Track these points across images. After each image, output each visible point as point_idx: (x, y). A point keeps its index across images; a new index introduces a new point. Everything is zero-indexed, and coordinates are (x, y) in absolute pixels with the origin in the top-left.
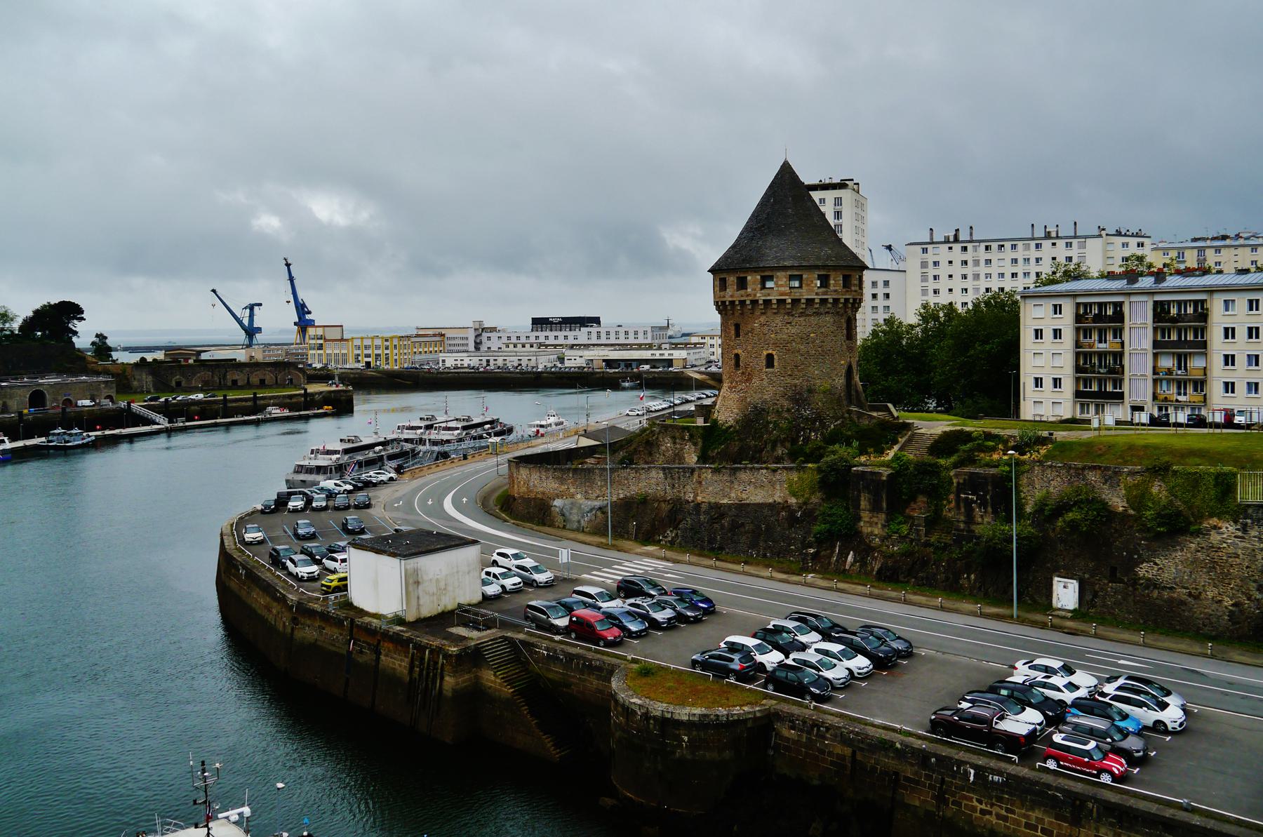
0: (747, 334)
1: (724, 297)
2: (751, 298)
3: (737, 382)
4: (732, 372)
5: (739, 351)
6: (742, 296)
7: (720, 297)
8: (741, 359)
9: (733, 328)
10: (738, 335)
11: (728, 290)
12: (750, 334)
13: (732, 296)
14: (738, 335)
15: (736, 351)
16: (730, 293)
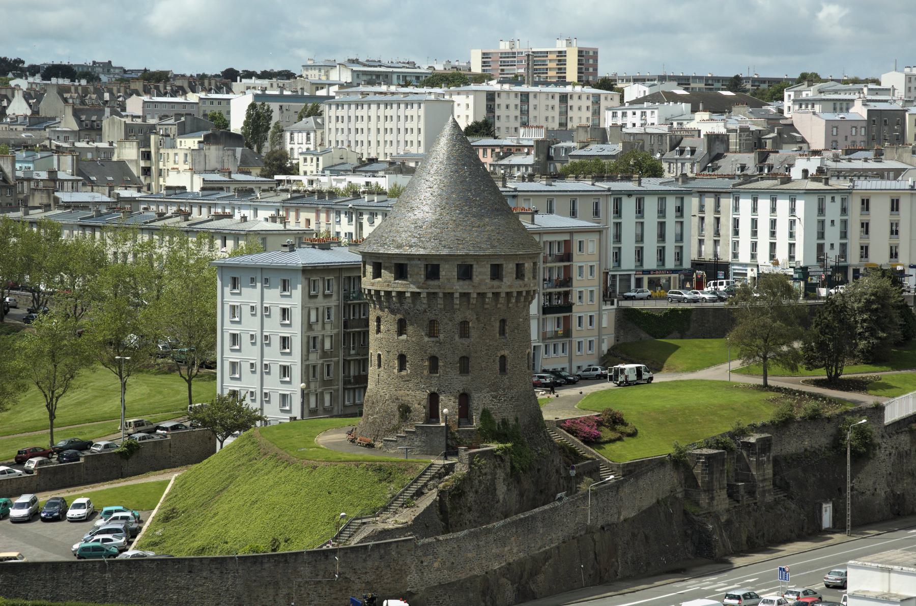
0: (513, 331)
1: (499, 287)
2: (527, 289)
3: (504, 390)
4: (495, 378)
5: (506, 352)
6: (521, 287)
7: (493, 287)
8: (509, 360)
9: (497, 325)
10: (502, 332)
11: (505, 280)
12: (516, 331)
13: (510, 286)
14: (502, 332)
15: (503, 353)
16: (509, 283)
